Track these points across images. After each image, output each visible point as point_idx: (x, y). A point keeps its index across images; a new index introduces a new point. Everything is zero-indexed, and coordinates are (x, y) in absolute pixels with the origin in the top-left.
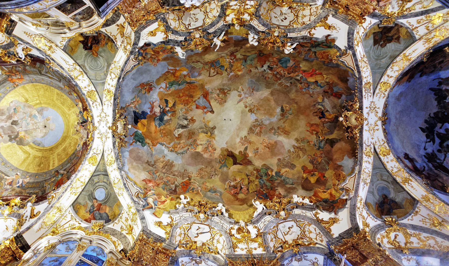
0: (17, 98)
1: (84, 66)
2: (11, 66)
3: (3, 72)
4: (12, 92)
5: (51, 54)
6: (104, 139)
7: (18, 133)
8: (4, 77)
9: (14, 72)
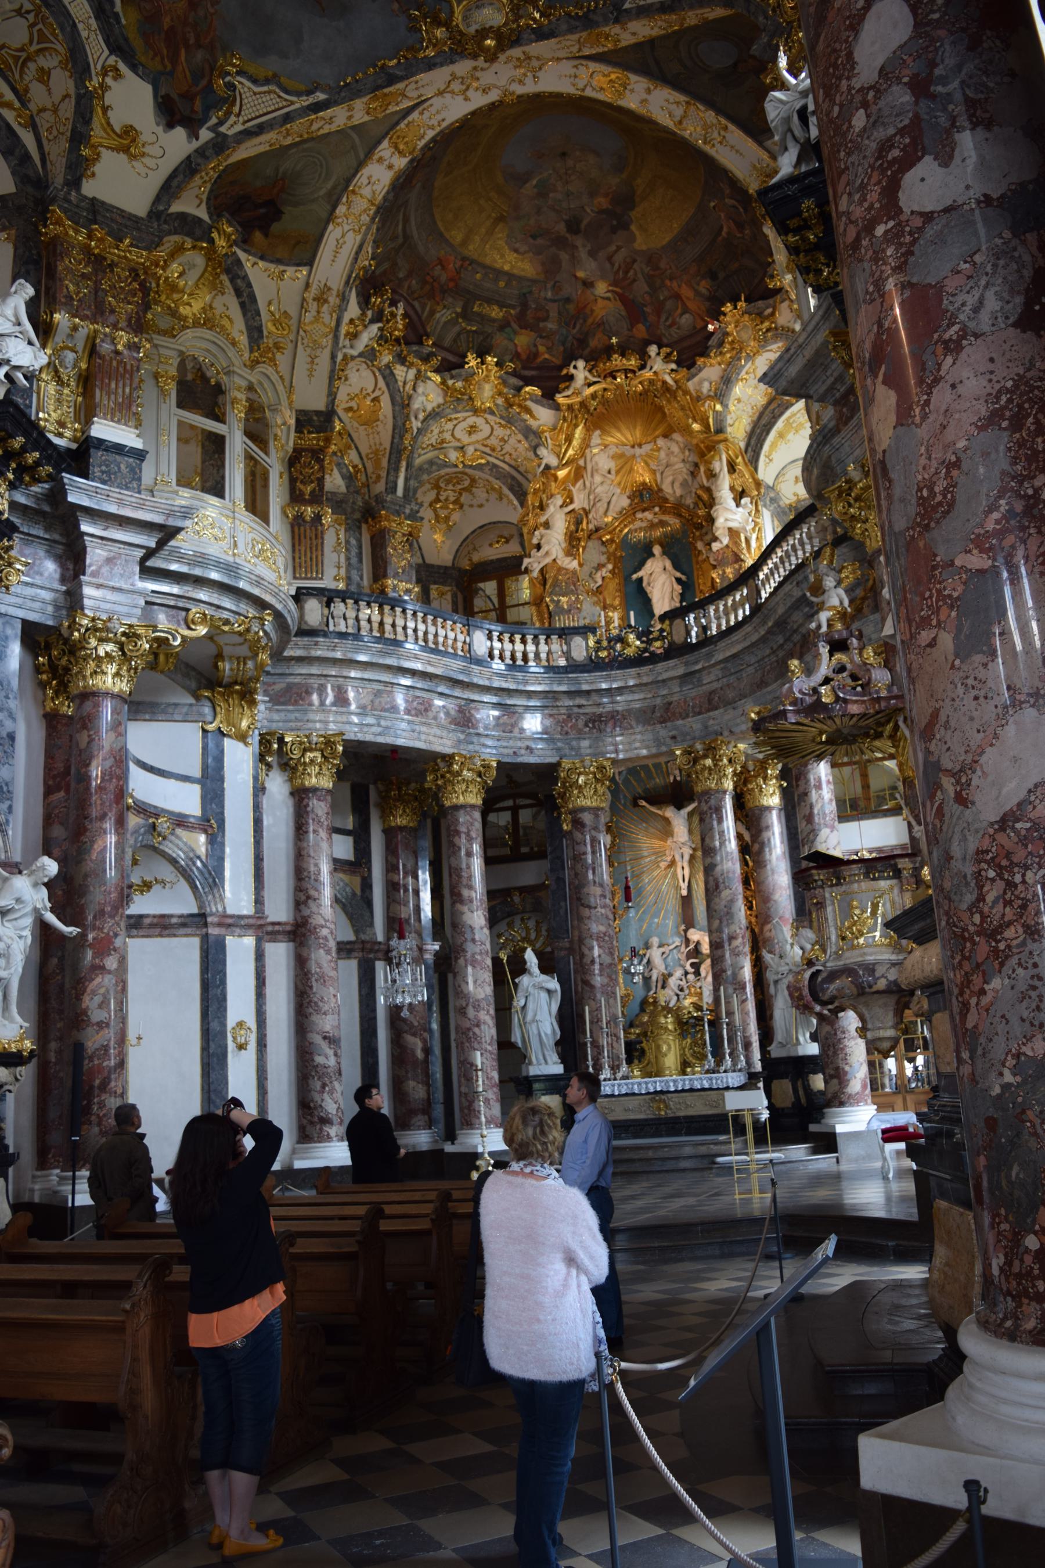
0: (501, 243)
1: (329, 194)
2: (416, 304)
3: (439, 308)
4: (488, 261)
5: (335, 293)
6: (535, 63)
7: (601, 212)
8: (450, 300)
9: (428, 287)
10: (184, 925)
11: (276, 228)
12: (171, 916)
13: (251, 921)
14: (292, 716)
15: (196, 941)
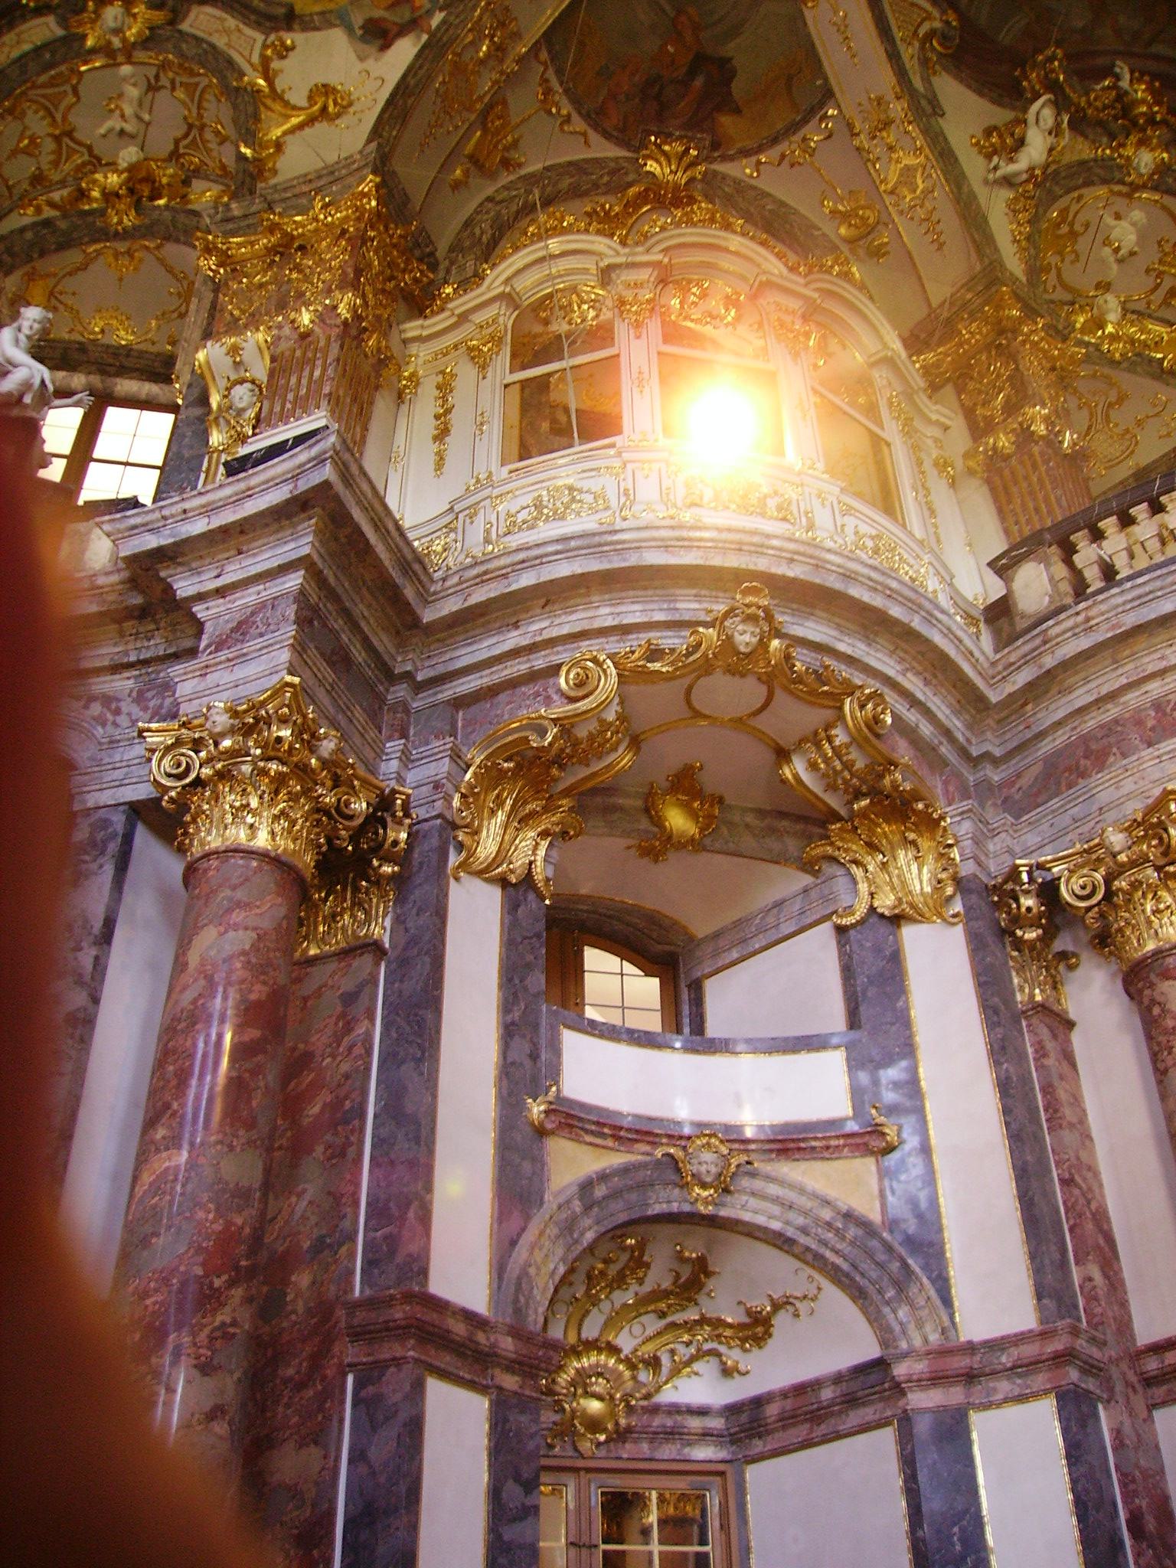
10: (851, 1401)
11: (739, 88)
12: (815, 1385)
13: (1029, 1351)
14: (1065, 820)
15: (886, 1439)
